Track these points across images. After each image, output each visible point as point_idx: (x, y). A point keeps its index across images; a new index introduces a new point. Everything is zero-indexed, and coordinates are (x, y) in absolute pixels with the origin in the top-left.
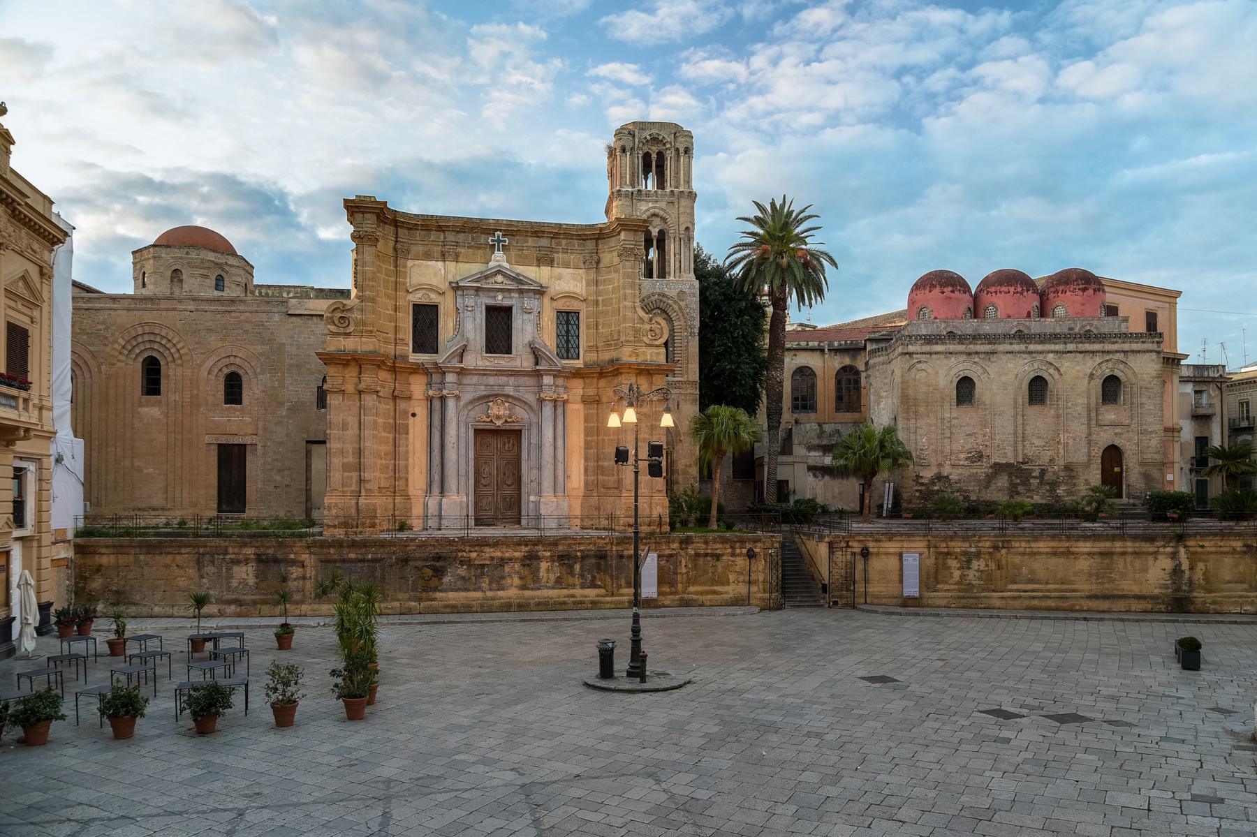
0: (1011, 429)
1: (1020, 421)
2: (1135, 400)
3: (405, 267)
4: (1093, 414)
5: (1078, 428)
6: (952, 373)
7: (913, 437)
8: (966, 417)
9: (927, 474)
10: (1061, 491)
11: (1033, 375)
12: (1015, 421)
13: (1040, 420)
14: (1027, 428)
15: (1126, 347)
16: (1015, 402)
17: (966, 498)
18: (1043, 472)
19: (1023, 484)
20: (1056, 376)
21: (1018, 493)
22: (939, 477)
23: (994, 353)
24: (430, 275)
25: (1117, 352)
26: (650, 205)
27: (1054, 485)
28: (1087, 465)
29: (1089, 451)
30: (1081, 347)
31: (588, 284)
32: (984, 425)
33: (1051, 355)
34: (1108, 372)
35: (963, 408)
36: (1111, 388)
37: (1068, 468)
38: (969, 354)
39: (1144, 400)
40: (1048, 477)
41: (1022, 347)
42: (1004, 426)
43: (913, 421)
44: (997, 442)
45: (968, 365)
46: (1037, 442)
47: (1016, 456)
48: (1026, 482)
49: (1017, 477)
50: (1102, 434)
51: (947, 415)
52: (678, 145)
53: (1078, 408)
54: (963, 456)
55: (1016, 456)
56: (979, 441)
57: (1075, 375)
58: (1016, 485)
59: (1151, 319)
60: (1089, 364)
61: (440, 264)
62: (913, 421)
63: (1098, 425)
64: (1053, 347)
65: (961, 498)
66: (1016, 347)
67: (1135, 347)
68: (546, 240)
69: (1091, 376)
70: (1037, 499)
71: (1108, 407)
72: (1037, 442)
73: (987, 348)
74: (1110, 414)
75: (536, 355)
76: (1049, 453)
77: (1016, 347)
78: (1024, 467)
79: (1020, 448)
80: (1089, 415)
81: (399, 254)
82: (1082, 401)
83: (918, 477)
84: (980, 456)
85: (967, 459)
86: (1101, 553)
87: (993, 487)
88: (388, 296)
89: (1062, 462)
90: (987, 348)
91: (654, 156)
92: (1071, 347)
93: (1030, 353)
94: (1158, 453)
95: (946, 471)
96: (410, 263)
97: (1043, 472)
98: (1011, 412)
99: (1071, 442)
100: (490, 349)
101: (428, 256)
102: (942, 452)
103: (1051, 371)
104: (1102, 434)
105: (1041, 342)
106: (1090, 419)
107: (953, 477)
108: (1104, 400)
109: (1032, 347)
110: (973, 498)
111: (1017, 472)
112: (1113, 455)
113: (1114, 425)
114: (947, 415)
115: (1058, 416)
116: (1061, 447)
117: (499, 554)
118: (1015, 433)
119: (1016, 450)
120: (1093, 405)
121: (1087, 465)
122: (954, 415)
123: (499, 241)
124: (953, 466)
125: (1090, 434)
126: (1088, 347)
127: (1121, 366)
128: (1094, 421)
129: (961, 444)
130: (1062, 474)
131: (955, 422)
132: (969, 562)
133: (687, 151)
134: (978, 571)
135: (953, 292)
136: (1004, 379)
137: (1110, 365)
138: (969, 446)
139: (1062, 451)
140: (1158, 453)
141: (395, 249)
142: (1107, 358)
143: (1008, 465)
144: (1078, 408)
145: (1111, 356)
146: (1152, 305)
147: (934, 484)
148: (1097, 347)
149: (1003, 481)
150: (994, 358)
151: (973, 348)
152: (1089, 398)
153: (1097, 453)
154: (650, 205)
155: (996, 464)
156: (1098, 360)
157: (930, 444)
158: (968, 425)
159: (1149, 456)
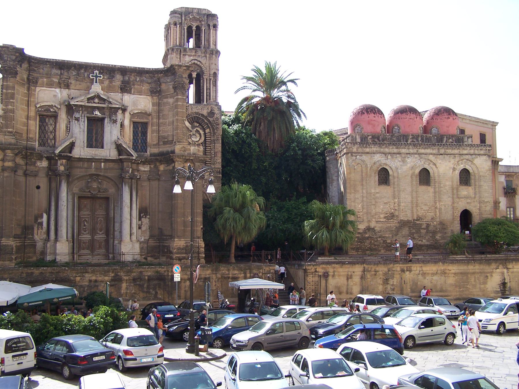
0: (409, 199)
2: (477, 183)
3: (35, 91)
4: (455, 191)
5: (447, 200)
7: (353, 204)
8: (385, 191)
9: (362, 227)
10: (438, 237)
12: (412, 195)
13: (426, 193)
14: (419, 199)
15: (472, 152)
17: (385, 242)
18: (428, 225)
23: (399, 153)
24: (49, 95)
26: (192, 58)
27: (434, 233)
29: (453, 212)
31: (153, 105)
33: (431, 156)
34: (462, 167)
36: (465, 177)
37: (441, 223)
38: (385, 154)
39: (482, 183)
40: (430, 228)
41: (415, 151)
42: (406, 198)
46: (425, 208)
48: (418, 231)
52: (209, 23)
54: (382, 216)
59: (483, 138)
61: (58, 90)
65: (382, 241)
67: (476, 152)
68: (126, 77)
70: (425, 242)
73: (395, 151)
74: (465, 191)
75: (119, 148)
76: (432, 214)
77: (411, 151)
78: (418, 222)
79: (415, 211)
81: (31, 82)
85: (385, 217)
86: (461, 273)
87: (400, 235)
88: (23, 110)
89: (438, 220)
90: (395, 151)
91: (194, 28)
92: (442, 151)
93: (420, 154)
95: (373, 225)
96: (38, 89)
98: (409, 189)
99: (443, 207)
100: (90, 145)
101: (50, 85)
102: (370, 213)
103: (431, 165)
104: (460, 203)
106: (453, 194)
108: (460, 183)
110: (389, 241)
111: (413, 226)
112: (466, 217)
113: (466, 197)
116: (437, 210)
117: (94, 278)
118: (412, 202)
119: (412, 212)
120: (455, 186)
123: (96, 77)
124: (377, 222)
125: (453, 203)
127: (470, 163)
128: (455, 195)
131: (378, 195)
132: (387, 280)
133: (215, 26)
134: (393, 285)
135: (375, 117)
138: (385, 210)
139: (438, 213)
141: (28, 79)
142: (462, 158)
143: (408, 222)
146: (483, 130)
147: (366, 233)
148: (456, 151)
149: (405, 231)
151: (387, 150)
152: (452, 182)
153: (458, 214)
154: (192, 58)
155: (401, 220)
157: (363, 208)
158: (385, 197)
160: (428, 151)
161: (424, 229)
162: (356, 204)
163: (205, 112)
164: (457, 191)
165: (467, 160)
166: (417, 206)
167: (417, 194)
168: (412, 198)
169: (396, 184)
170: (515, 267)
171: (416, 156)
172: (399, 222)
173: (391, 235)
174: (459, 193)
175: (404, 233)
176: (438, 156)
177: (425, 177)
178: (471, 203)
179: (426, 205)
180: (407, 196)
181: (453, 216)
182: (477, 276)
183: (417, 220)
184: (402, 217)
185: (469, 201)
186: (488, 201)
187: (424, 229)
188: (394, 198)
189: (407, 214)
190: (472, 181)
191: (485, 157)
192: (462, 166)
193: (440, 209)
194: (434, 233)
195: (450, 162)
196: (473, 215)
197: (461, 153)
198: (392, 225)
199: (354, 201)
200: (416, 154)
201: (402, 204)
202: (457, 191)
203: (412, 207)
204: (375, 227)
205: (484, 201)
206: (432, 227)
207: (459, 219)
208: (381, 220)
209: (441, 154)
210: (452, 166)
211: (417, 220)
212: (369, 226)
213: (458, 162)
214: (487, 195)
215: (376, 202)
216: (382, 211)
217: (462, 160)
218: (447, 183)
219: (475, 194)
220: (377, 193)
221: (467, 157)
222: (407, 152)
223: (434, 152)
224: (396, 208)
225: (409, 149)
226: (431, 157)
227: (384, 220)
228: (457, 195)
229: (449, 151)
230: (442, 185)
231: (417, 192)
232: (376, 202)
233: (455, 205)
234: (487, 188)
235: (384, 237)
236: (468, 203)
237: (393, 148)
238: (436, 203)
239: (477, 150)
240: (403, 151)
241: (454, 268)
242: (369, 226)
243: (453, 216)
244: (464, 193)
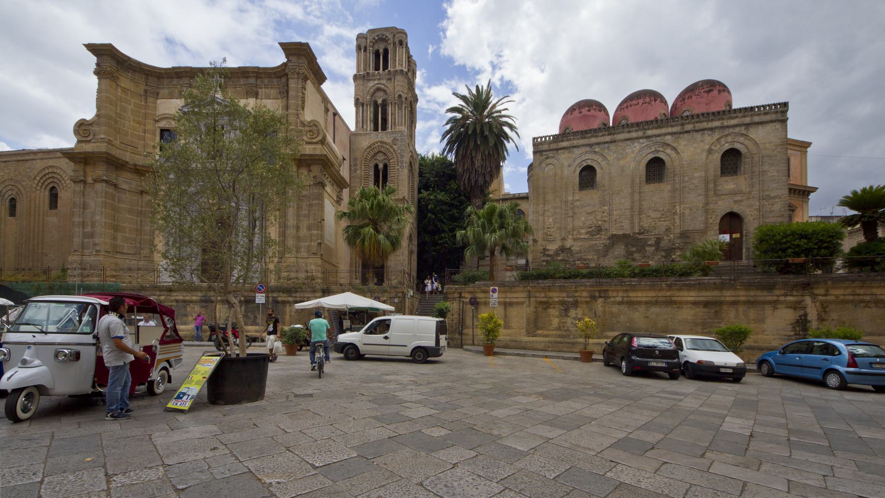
0: (627, 204)
2: (756, 169)
4: (711, 186)
5: (695, 199)
6: (577, 162)
9: (553, 247)
10: (676, 255)
11: (651, 156)
13: (658, 195)
14: (644, 203)
15: (747, 120)
16: (633, 181)
18: (658, 240)
19: (638, 251)
20: (673, 154)
21: (634, 260)
22: (563, 249)
28: (703, 232)
29: (706, 219)
30: (699, 126)
32: (603, 203)
33: (669, 137)
34: (727, 147)
35: (584, 192)
37: (684, 235)
38: (591, 145)
39: (766, 168)
40: (664, 244)
41: (640, 134)
42: (622, 203)
43: (541, 206)
44: (614, 217)
45: (588, 156)
47: (633, 228)
48: (641, 249)
49: (633, 246)
50: (720, 203)
51: (570, 198)
53: (696, 181)
54: (583, 231)
55: (633, 228)
57: (694, 153)
58: (631, 254)
60: (709, 139)
62: (541, 206)
63: (716, 194)
64: (670, 130)
66: (634, 135)
67: (756, 119)
69: (710, 151)
71: (725, 178)
72: (653, 215)
74: (729, 184)
77: (634, 135)
79: (636, 221)
80: (706, 186)
83: (545, 249)
84: (599, 230)
85: (587, 233)
89: (678, 231)
92: (689, 127)
94: (782, 216)
95: (568, 243)
97: (658, 240)
99: (687, 212)
102: (565, 228)
103: (669, 151)
104: (720, 203)
105: (656, 128)
106: (707, 190)
107: (575, 249)
109: (649, 133)
110: (593, 265)
111: (632, 242)
113: (733, 193)
114: (570, 198)
115: (674, 190)
118: (632, 209)
121: (703, 232)
122: (577, 198)
124: (575, 240)
125: (707, 204)
126: (705, 125)
127: (742, 139)
129: (583, 220)
130: (678, 241)
131: (578, 203)
136: (622, 163)
137: (729, 139)
138: (588, 223)
139: (677, 221)
140: (782, 216)
142: (726, 132)
143: (625, 236)
144: (696, 181)
145: (731, 130)
148: (717, 124)
149: (620, 250)
150: (613, 147)
152: (706, 171)
155: (613, 236)
158: (589, 205)
159: (772, 220)
160: (664, 131)
161: (651, 245)
164: (715, 185)
166: (640, 213)
167: (640, 197)
168: (633, 202)
172: (609, 238)
173: (596, 257)
178: (740, 201)
179: (656, 211)
180: (623, 200)
181: (707, 223)
182: (741, 308)
185: (738, 198)
186: (774, 197)
187: (651, 245)
188: (604, 205)
193: (682, 215)
194: (670, 251)
195: (702, 141)
196: (746, 221)
197: (726, 123)
199: (544, 214)
200: (641, 138)
201: (615, 213)
202: (715, 185)
204: (573, 246)
206: (667, 241)
207: (717, 228)
210: (707, 147)
211: (639, 234)
212: (563, 246)
213: (718, 140)
214: (775, 185)
215: (574, 213)
216: (584, 224)
217: (727, 136)
218: (696, 175)
221: (737, 130)
222: (627, 136)
223: (675, 129)
225: (629, 132)
226: (668, 138)
227: (586, 236)
228: (715, 191)
229: (705, 125)
230: (686, 179)
231: (640, 193)
232: (574, 213)
233: (712, 206)
235: (585, 260)
236: (735, 202)
239: (759, 115)
241: (692, 294)
242: (563, 246)
243: (707, 223)
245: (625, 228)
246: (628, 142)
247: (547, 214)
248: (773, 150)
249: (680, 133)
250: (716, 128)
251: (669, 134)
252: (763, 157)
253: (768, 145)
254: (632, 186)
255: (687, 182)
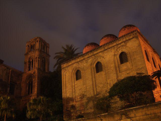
1: (94, 80)
4: (118, 69)
13: (101, 76)
14: (97, 81)
15: (124, 40)
23: (84, 59)
25: (121, 43)
33: (100, 53)
34: (120, 52)
38: (77, 62)
41: (92, 54)
46: (101, 86)
47: (94, 93)
54: (79, 97)
56: (83, 91)
67: (127, 39)
69: (115, 55)
73: (82, 58)
74: (124, 67)
76: (105, 89)
77: (90, 55)
78: (97, 96)
79: (95, 89)
80: (116, 69)
82: (113, 65)
85: (80, 98)
90: (82, 58)
92: (106, 48)
93: (94, 55)
98: (90, 77)
99: (111, 82)
104: (122, 75)
113: (126, 70)
115: (106, 74)
118: (93, 84)
120: (117, 65)
143: (92, 97)
145: (119, 45)
152: (115, 63)
155: (88, 97)
156: (116, 49)
162: (67, 94)
163: (32, 73)
165: (122, 46)
168: (93, 82)
169: (84, 76)
170: (137, 115)
171: (93, 57)
172: (87, 99)
174: (121, 69)
175: (90, 105)
176: (105, 51)
177: (99, 67)
179: (101, 84)
183: (97, 95)
184: (88, 96)
185: (128, 72)
189: (91, 93)
190: (129, 58)
191: (134, 39)
192: (120, 51)
197: (118, 43)
198: (83, 102)
201: (88, 87)
203: (93, 87)
205: (139, 68)
208: (78, 100)
209: (106, 50)
210: (113, 54)
211: (97, 95)
213: (116, 50)
216: (79, 94)
218: (112, 66)
219: (132, 66)
220: (76, 85)
221: (122, 44)
224: (85, 91)
225: (88, 54)
230: (109, 68)
234: (139, 58)
236: (128, 74)
237: (81, 58)
238: (107, 80)
240: (86, 57)
244: (124, 68)
245: (90, 94)
246: (88, 58)
247: (67, 92)
248: (136, 49)
249: (104, 51)
250: (115, 46)
251: (100, 52)
252: (133, 52)
253: (134, 47)
254: (92, 75)
255: (109, 69)
